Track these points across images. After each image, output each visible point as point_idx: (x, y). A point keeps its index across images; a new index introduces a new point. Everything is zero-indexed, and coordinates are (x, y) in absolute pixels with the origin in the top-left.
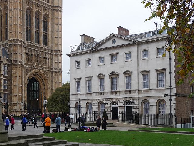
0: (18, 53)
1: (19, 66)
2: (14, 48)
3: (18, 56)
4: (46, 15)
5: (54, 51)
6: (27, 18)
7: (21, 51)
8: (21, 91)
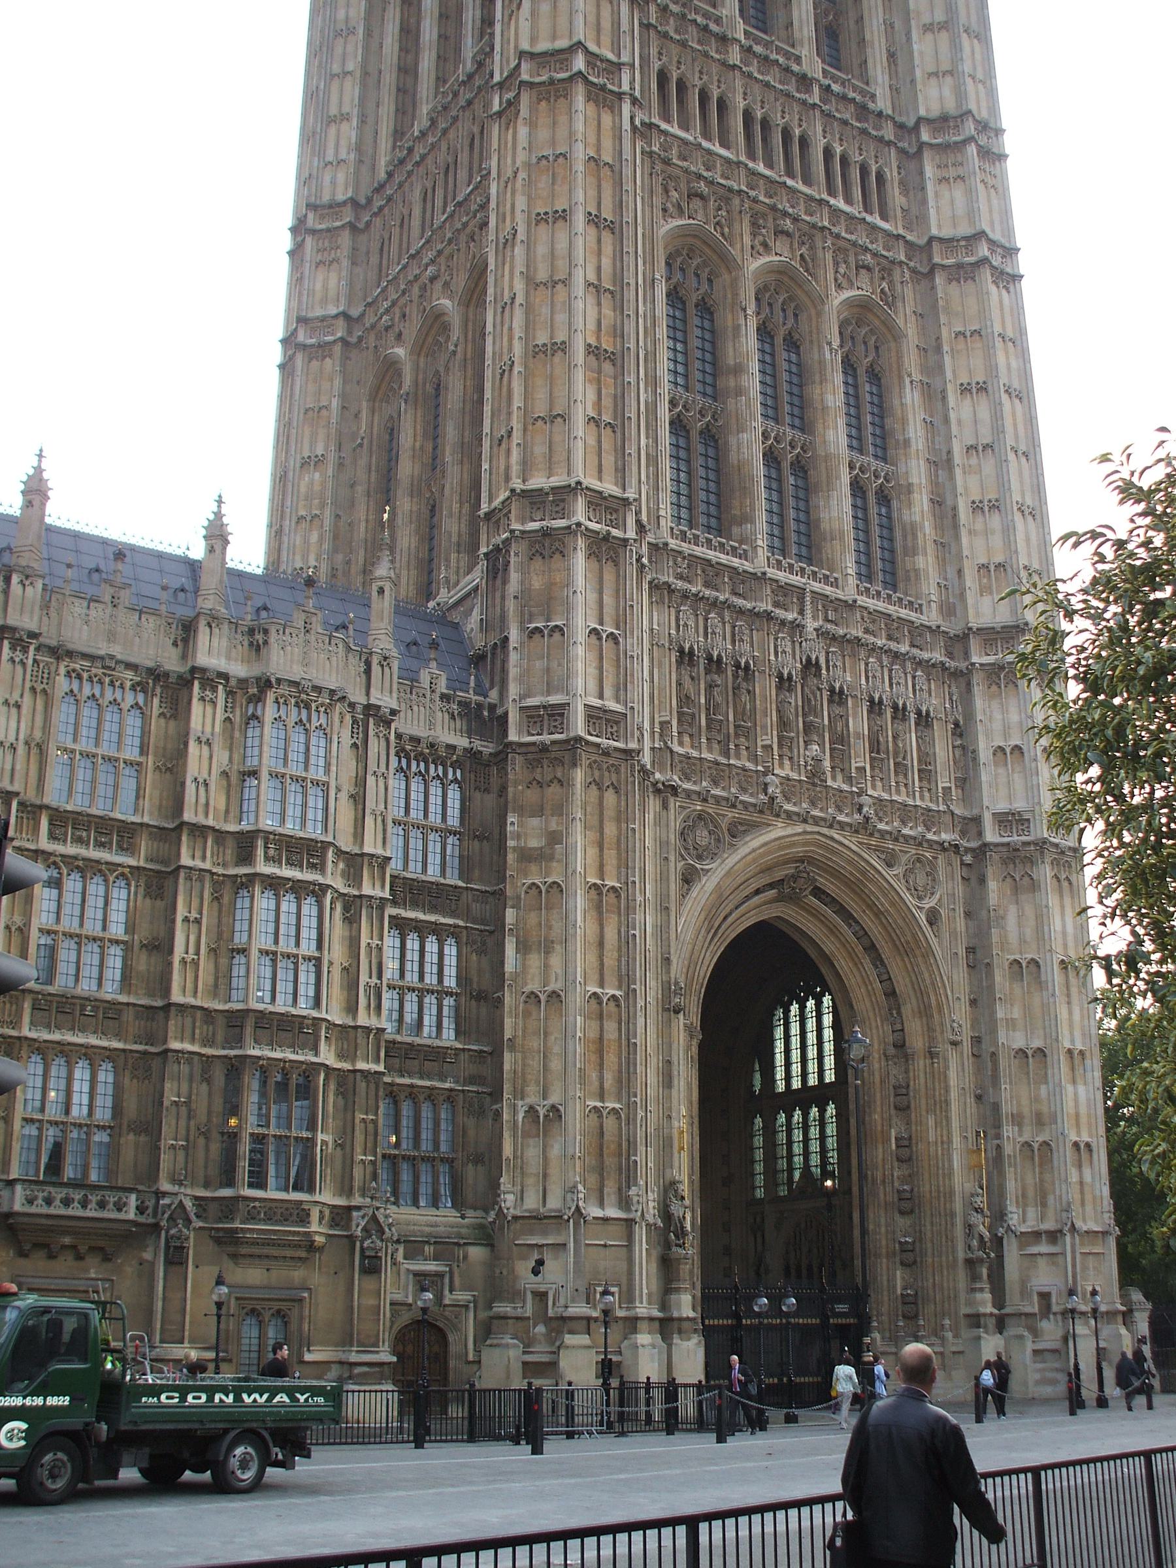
0: (582, 621)
1: (585, 759)
2: (537, 583)
3: (581, 655)
4: (860, 312)
5: (974, 644)
6: (678, 331)
7: (608, 600)
8: (611, 1059)
